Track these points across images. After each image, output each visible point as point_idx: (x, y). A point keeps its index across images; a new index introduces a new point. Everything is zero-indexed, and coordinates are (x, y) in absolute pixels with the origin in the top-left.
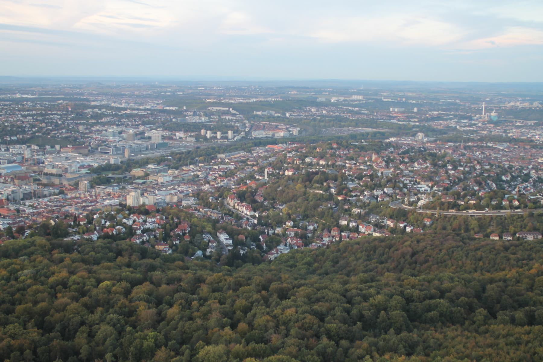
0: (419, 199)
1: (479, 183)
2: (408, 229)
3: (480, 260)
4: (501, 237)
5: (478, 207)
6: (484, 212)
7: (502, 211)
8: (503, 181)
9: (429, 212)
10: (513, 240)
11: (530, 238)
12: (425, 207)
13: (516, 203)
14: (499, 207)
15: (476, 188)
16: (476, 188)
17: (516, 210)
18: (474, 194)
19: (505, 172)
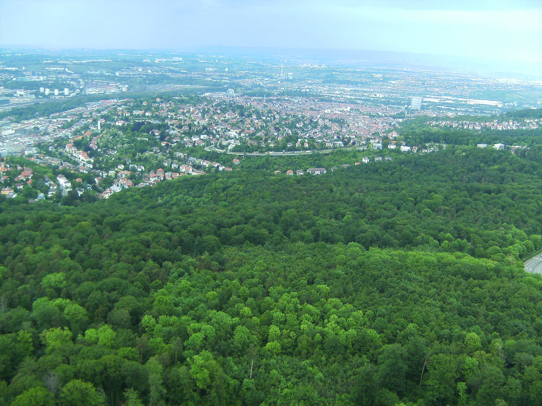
0: (229, 144)
1: (277, 129)
2: (221, 169)
3: (277, 192)
4: (295, 173)
5: (276, 149)
6: (282, 153)
7: (295, 152)
8: (297, 128)
9: (238, 154)
10: (305, 175)
11: (317, 173)
12: (234, 150)
13: (307, 145)
14: (293, 149)
15: (276, 134)
16: (276, 134)
17: (307, 151)
18: (273, 139)
19: (298, 121)
